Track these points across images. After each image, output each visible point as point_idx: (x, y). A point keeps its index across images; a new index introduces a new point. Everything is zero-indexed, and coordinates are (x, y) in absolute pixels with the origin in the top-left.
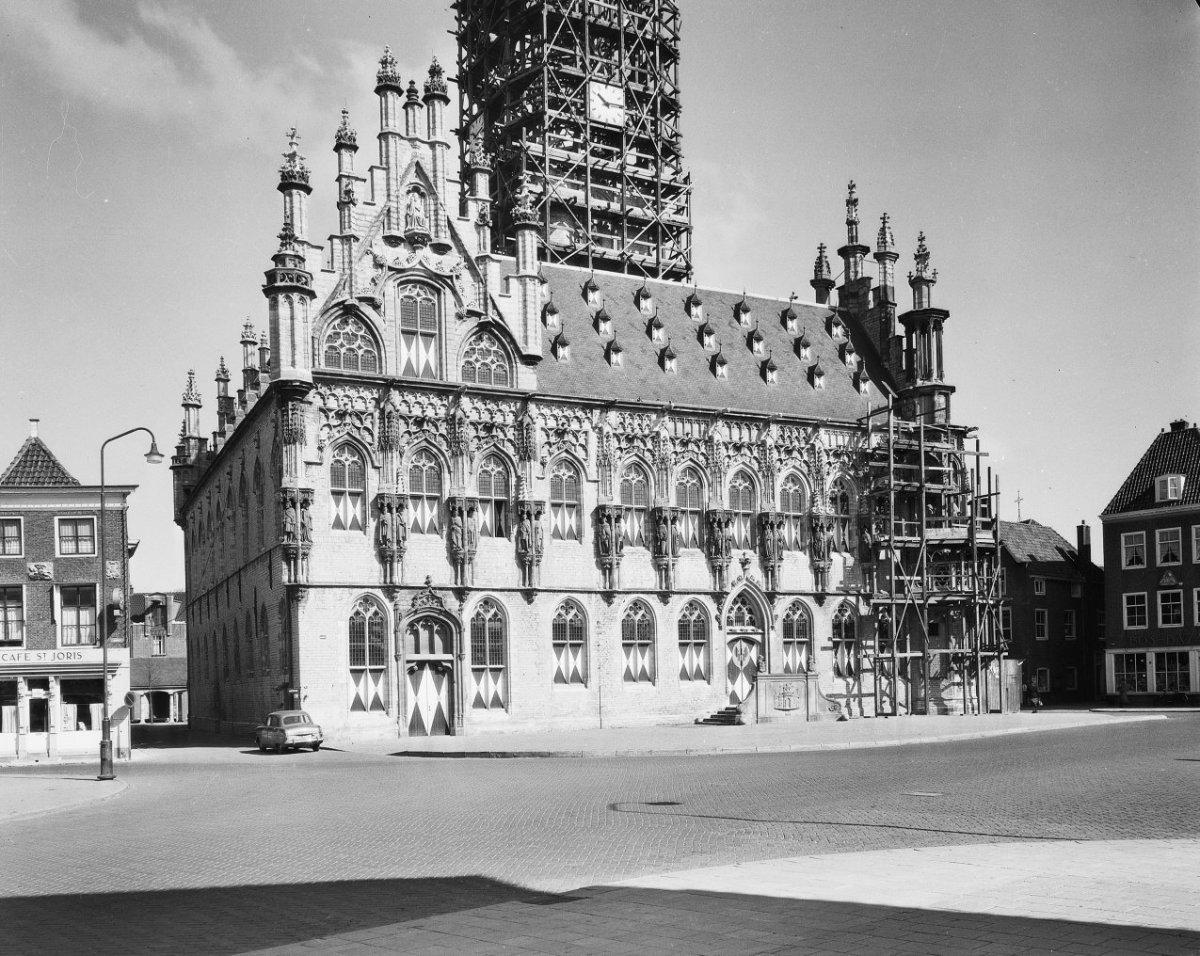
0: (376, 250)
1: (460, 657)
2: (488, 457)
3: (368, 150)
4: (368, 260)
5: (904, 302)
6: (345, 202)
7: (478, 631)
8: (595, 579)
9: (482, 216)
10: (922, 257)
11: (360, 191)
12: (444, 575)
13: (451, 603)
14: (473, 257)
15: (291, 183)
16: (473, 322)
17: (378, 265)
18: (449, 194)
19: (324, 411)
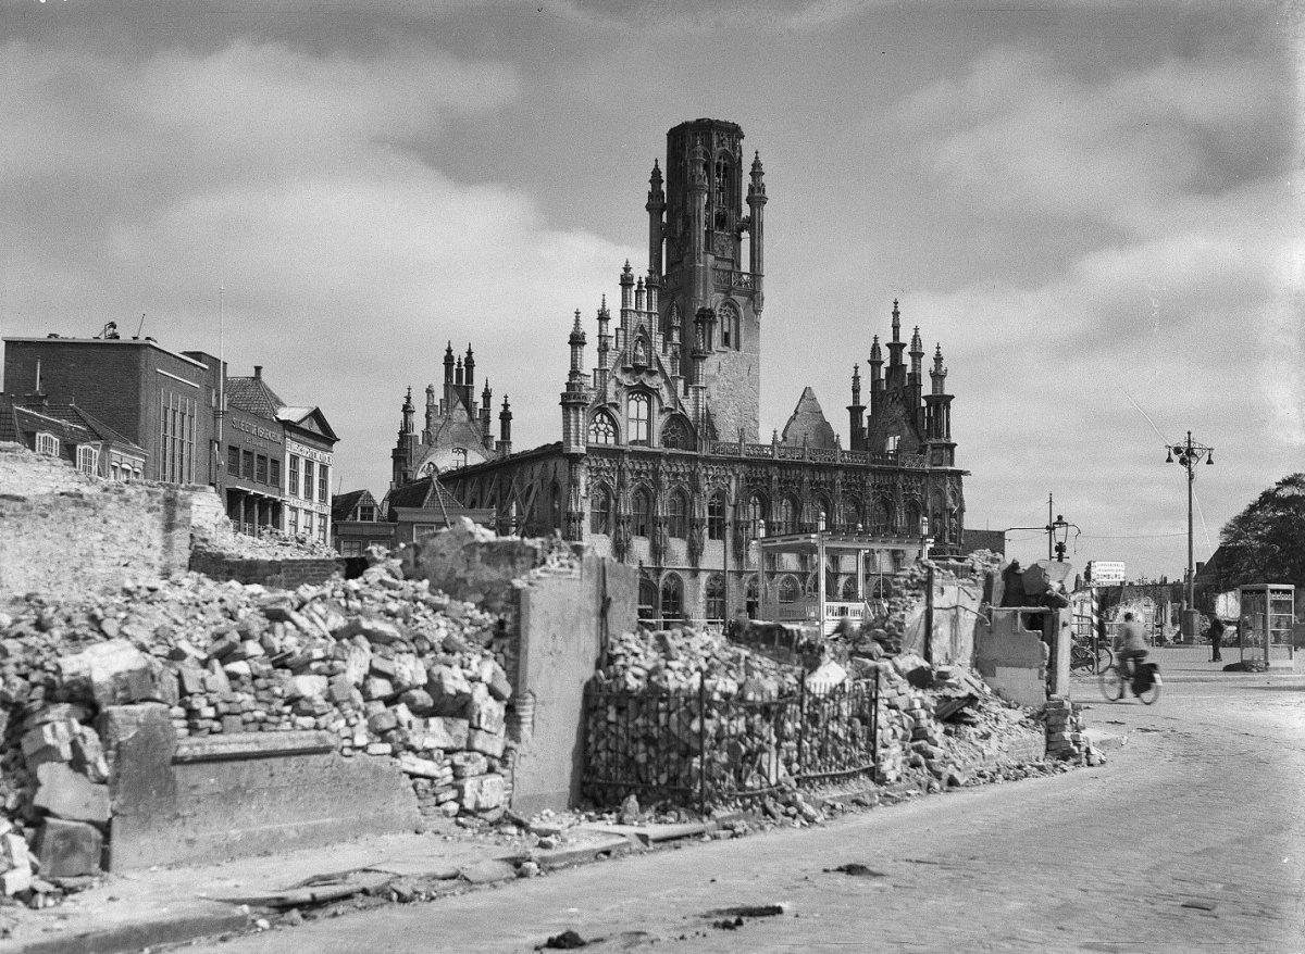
0: (618, 375)
1: (656, 608)
2: (674, 493)
3: (615, 321)
4: (613, 382)
5: (927, 389)
6: (603, 349)
7: (666, 593)
8: (731, 565)
9: (675, 353)
10: (938, 359)
11: (612, 343)
12: (648, 563)
13: (652, 577)
14: (669, 376)
15: (577, 341)
16: (667, 414)
17: (619, 384)
18: (658, 340)
19: (589, 468)
